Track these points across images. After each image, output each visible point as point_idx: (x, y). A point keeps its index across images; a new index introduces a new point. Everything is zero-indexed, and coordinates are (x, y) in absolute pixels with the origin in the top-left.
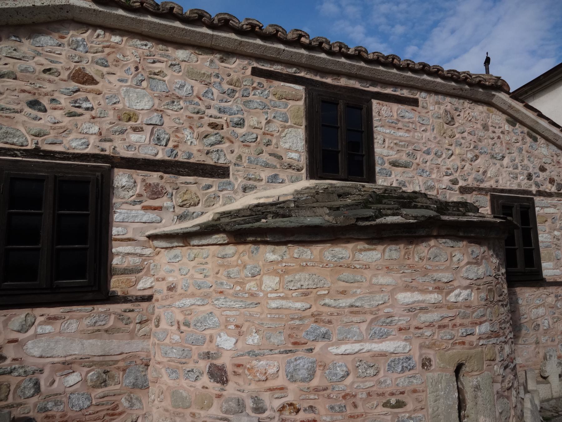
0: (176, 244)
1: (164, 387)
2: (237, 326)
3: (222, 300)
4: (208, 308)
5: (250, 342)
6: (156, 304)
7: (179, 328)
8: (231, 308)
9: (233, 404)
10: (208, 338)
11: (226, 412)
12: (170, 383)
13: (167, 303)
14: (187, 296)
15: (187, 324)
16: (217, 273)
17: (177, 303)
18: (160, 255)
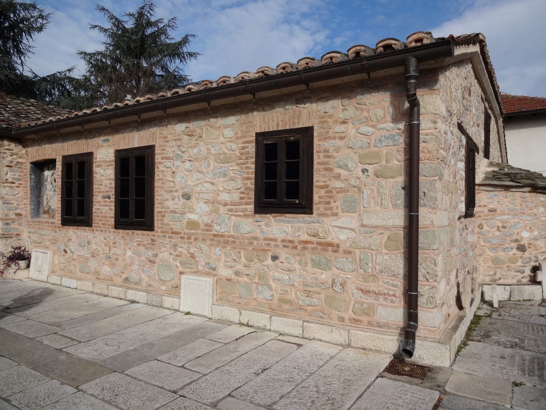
0: (499, 190)
1: (488, 257)
2: (530, 228)
3: (524, 217)
4: (516, 220)
5: (535, 234)
6: (479, 218)
7: (498, 229)
8: (528, 220)
9: (528, 260)
10: (516, 233)
11: (526, 263)
12: (492, 254)
13: (489, 217)
14: (504, 215)
15: (504, 227)
16: (521, 205)
17: (498, 218)
18: (481, 194)
